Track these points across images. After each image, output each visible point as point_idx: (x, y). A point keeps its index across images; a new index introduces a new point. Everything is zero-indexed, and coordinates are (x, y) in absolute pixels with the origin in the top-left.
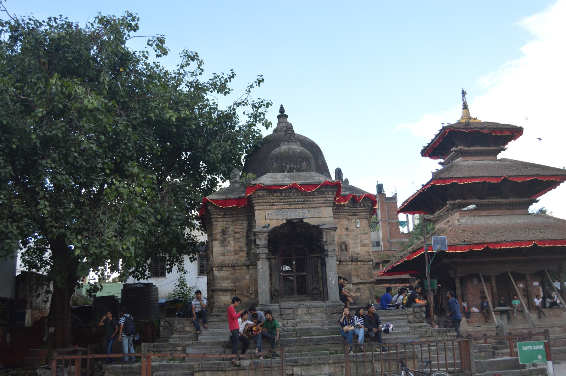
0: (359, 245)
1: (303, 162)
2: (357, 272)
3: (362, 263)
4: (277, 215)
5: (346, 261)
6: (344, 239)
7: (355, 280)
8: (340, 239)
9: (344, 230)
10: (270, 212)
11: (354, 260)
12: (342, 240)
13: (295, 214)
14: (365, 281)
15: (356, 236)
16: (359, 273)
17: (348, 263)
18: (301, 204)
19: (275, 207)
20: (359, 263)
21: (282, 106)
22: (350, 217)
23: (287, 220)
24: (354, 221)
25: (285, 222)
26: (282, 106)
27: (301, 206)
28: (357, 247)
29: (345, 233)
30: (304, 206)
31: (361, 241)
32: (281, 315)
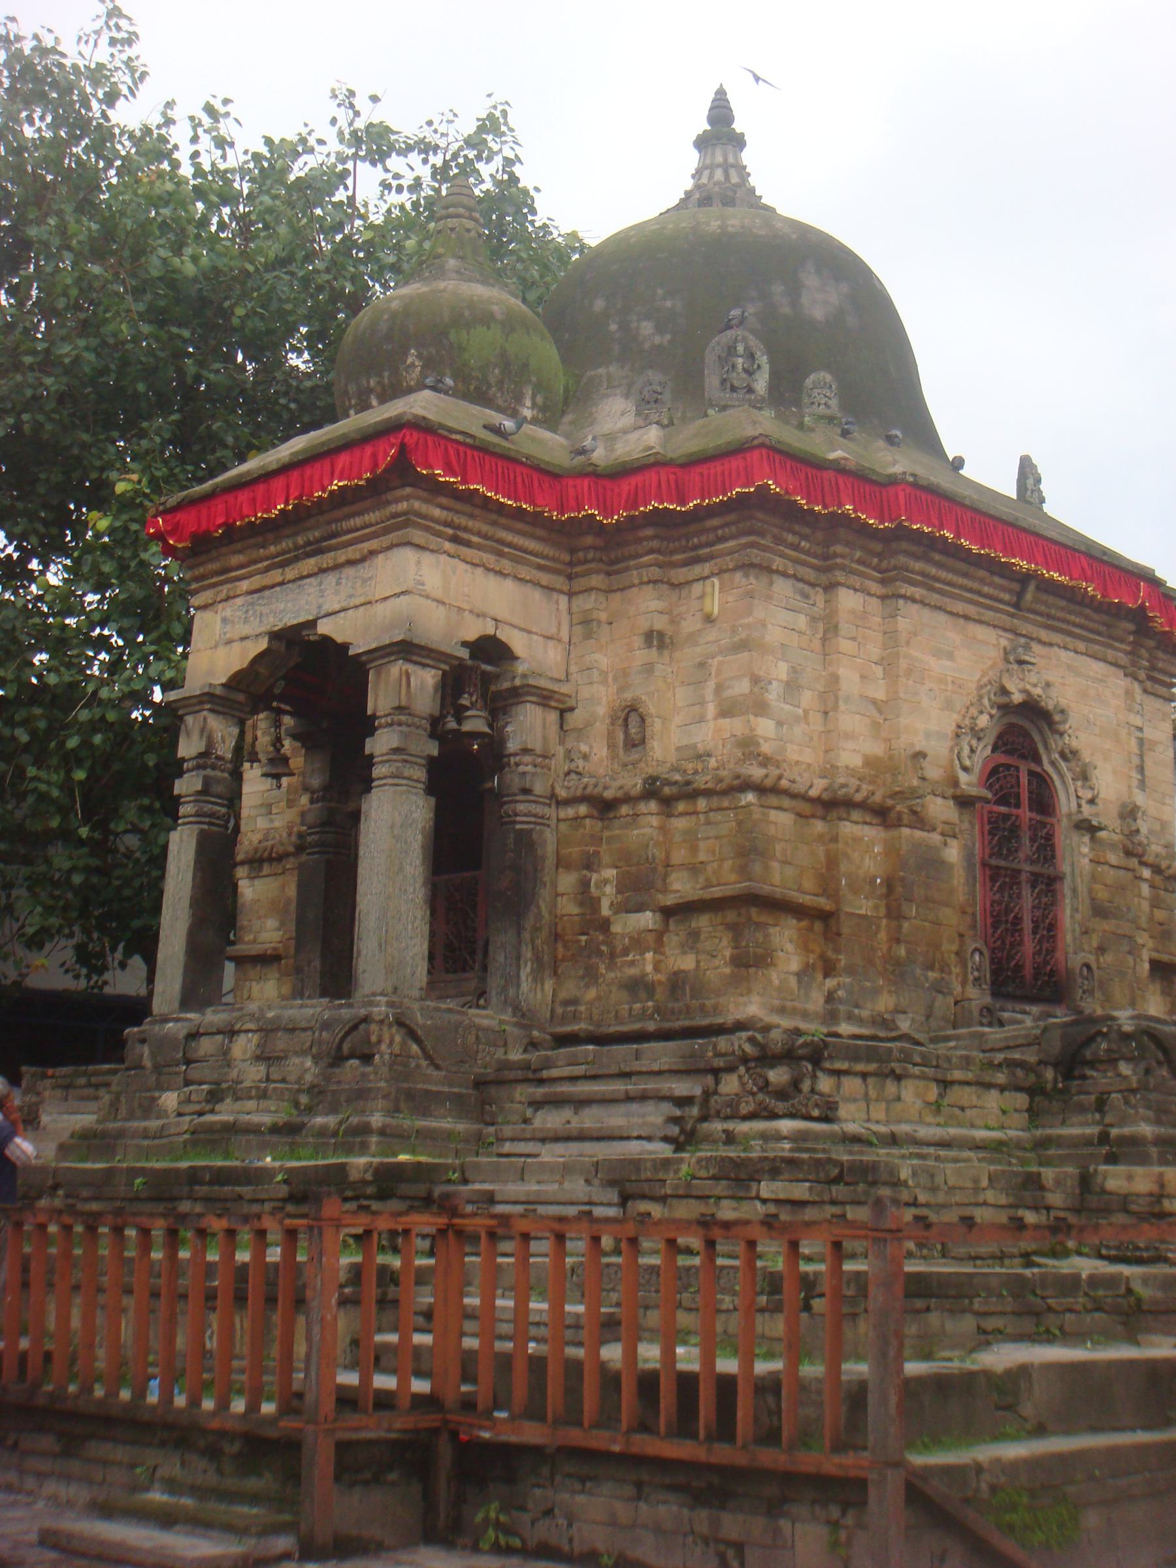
0: (711, 709)
1: (406, 354)
2: (694, 850)
3: (715, 802)
4: (246, 621)
5: (628, 799)
6: (638, 690)
7: (682, 887)
8: (621, 690)
9: (638, 641)
10: (228, 613)
11: (665, 794)
12: (628, 695)
13: (292, 606)
14: (717, 892)
15: (702, 665)
16: (702, 857)
17: (642, 807)
18: (309, 555)
19: (245, 585)
20: (702, 804)
21: (721, 94)
22: (681, 574)
23: (274, 636)
24: (697, 588)
25: (263, 644)
26: (721, 94)
27: (310, 564)
28: (702, 719)
29: (642, 655)
30: (327, 559)
31: (719, 689)
32: (188, 1062)
